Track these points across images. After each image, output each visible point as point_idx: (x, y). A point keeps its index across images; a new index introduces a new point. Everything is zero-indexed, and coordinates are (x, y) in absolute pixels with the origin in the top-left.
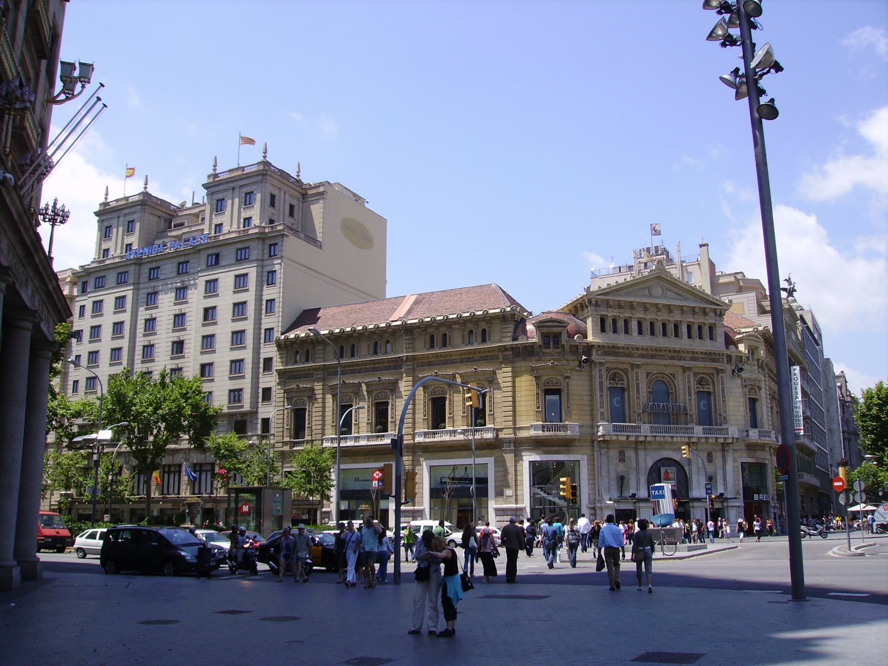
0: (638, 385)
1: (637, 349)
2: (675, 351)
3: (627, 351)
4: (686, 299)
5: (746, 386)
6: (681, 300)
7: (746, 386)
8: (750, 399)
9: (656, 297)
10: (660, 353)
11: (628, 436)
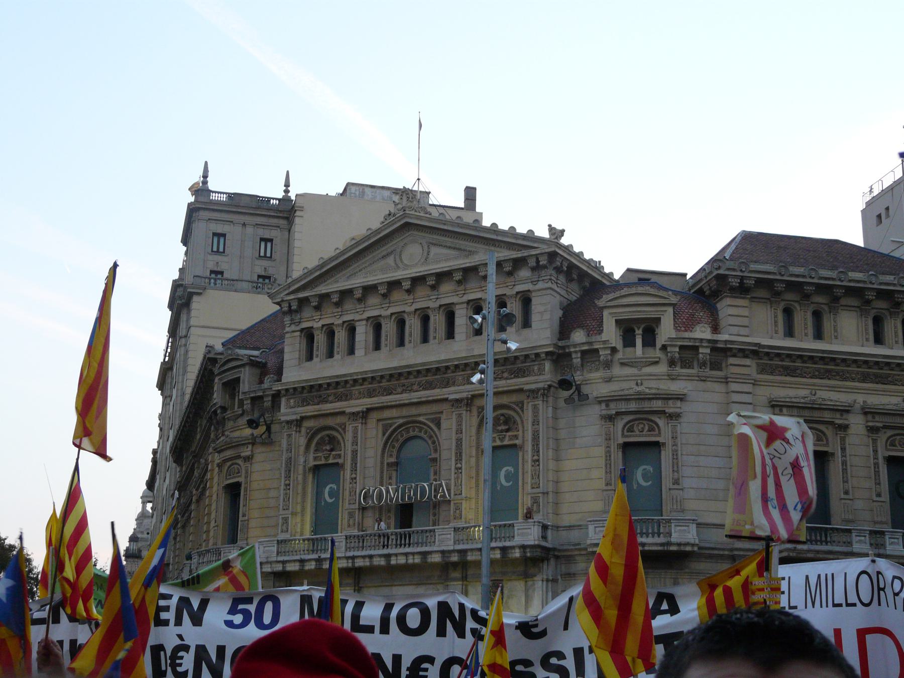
0: (355, 453)
1: (355, 381)
2: (428, 370)
3: (339, 387)
4: (471, 253)
5: (610, 418)
6: (456, 258)
7: (610, 418)
8: (626, 447)
9: (407, 267)
10: (403, 381)
11: (302, 561)
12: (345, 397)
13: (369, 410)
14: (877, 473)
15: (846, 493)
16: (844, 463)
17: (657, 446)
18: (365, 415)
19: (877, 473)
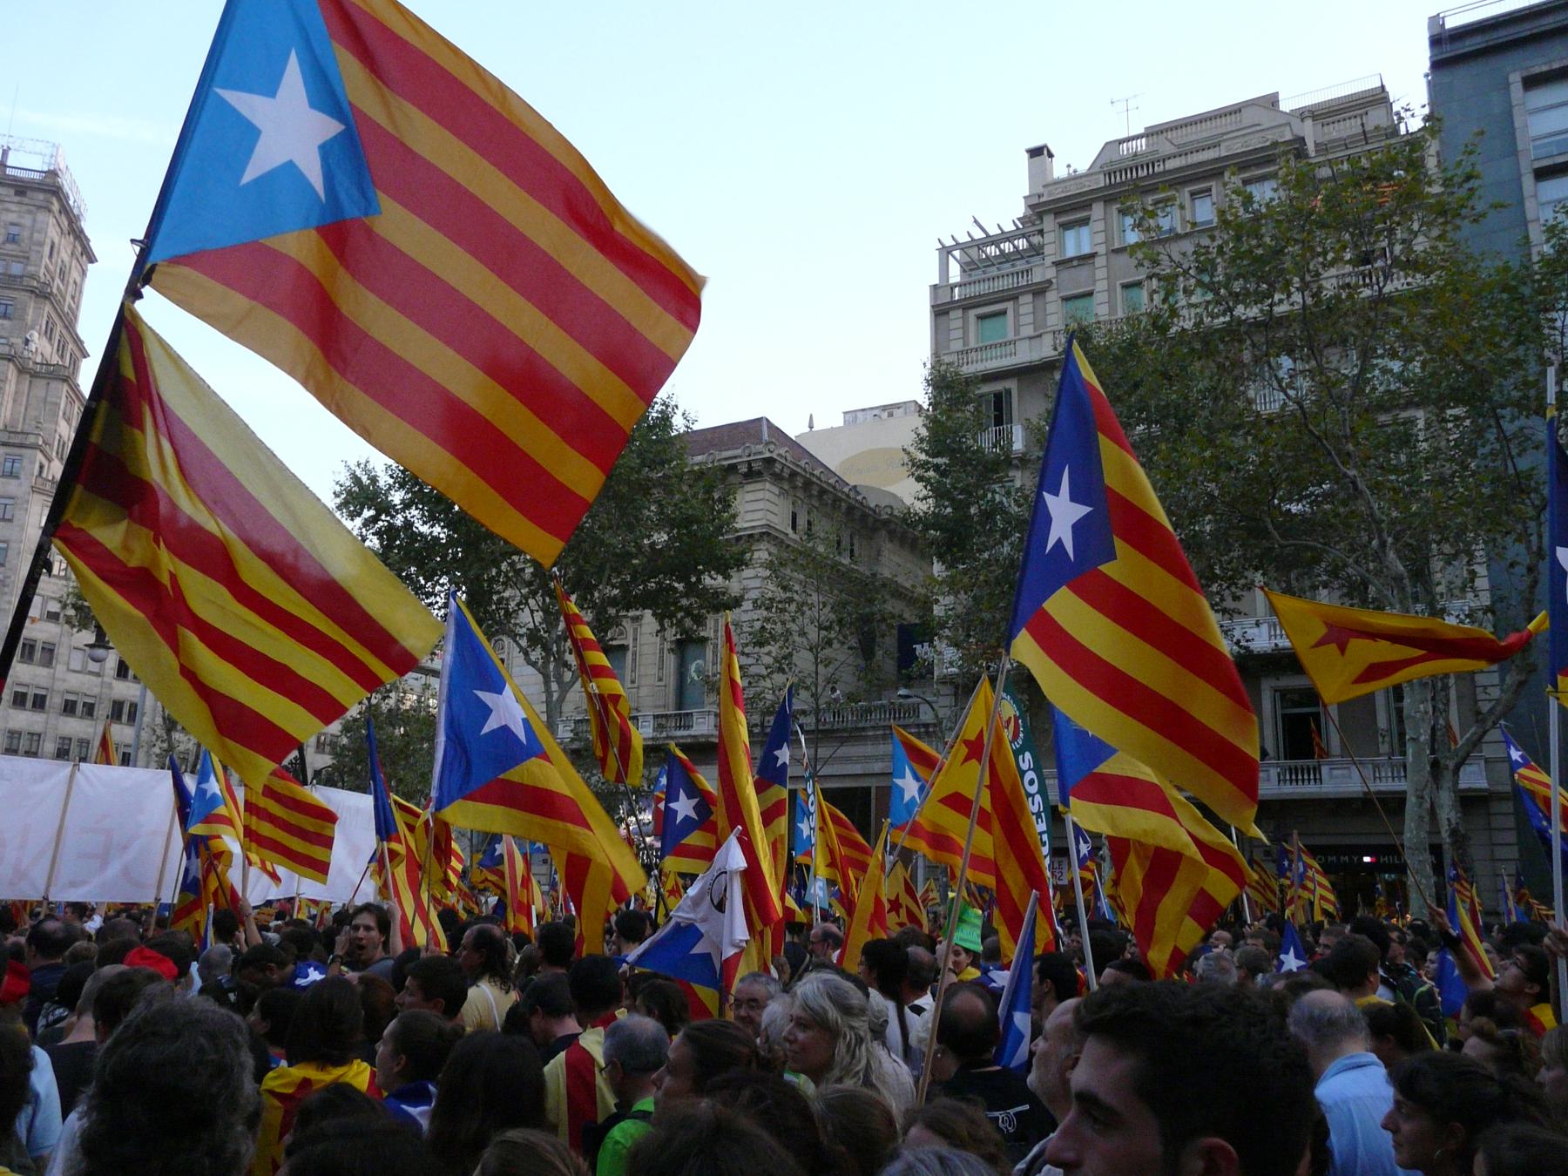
15: (633, 682)
16: (634, 654)
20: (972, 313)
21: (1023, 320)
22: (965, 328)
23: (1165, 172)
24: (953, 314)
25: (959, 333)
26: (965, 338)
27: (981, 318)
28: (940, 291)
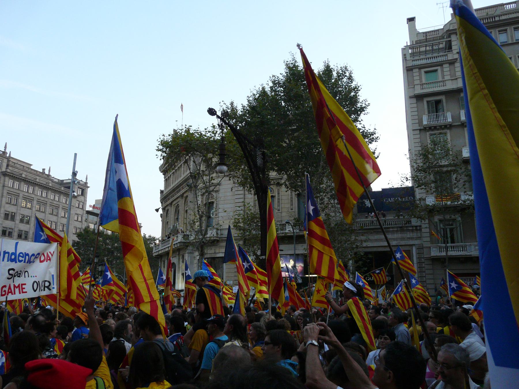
12: (169, 199)
13: (172, 202)
14: (292, 201)
16: (278, 199)
17: (213, 203)
18: (171, 204)
19: (292, 201)
20: (423, 71)
21: (445, 73)
22: (420, 75)
23: (500, 21)
24: (414, 71)
25: (418, 78)
26: (420, 79)
27: (426, 72)
28: (408, 62)
